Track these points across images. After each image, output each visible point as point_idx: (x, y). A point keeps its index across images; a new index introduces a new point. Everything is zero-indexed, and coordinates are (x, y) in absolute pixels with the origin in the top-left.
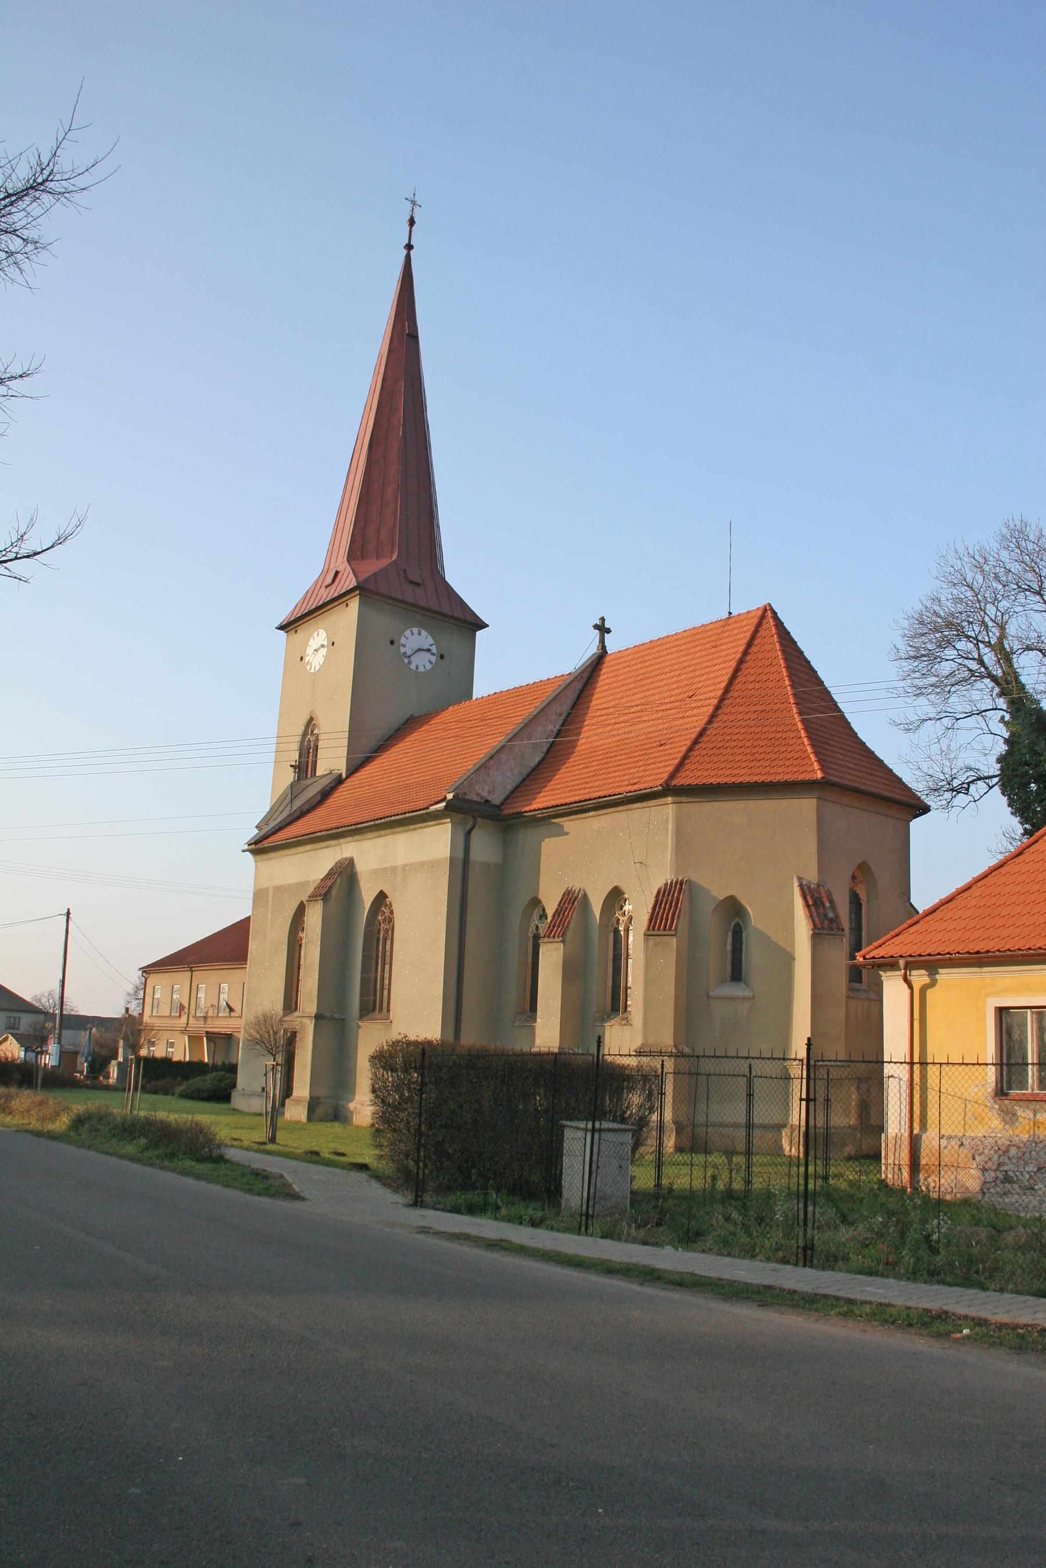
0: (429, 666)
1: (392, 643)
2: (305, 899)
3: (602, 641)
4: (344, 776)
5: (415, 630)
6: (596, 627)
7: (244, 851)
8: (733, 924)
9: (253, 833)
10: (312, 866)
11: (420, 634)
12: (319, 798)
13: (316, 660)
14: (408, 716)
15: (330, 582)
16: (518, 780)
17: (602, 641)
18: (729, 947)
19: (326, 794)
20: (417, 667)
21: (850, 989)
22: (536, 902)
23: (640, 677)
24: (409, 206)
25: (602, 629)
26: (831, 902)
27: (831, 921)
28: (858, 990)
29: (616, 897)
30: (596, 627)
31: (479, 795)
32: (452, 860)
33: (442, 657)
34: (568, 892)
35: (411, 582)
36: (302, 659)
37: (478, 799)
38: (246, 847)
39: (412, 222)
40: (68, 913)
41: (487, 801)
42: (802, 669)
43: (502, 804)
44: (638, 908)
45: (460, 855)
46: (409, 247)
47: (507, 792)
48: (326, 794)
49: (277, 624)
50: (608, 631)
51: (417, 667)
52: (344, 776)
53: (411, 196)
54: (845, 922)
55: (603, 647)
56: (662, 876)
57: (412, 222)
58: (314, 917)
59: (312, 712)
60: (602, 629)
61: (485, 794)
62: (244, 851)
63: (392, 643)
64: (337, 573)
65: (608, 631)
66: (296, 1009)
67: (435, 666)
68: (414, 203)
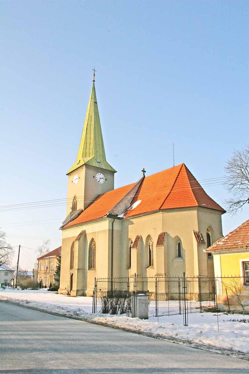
0: (103, 182)
1: (94, 177)
2: (74, 240)
4: (83, 210)
5: (99, 174)
6: (142, 171)
8: (178, 243)
9: (62, 225)
10: (75, 232)
11: (100, 174)
12: (77, 215)
15: (78, 163)
18: (177, 249)
19: (79, 214)
25: (144, 171)
26: (202, 236)
27: (202, 241)
29: (149, 237)
30: (142, 171)
31: (115, 213)
32: (109, 230)
33: (106, 180)
35: (98, 162)
36: (72, 182)
38: (60, 228)
39: (94, 75)
44: (155, 240)
45: (111, 228)
48: (79, 214)
50: (145, 172)
52: (83, 210)
54: (206, 241)
55: (144, 176)
56: (160, 232)
58: (77, 244)
59: (75, 195)
60: (144, 171)
63: (94, 177)
64: (80, 161)
65: (145, 172)
66: (73, 268)
68: (94, 70)
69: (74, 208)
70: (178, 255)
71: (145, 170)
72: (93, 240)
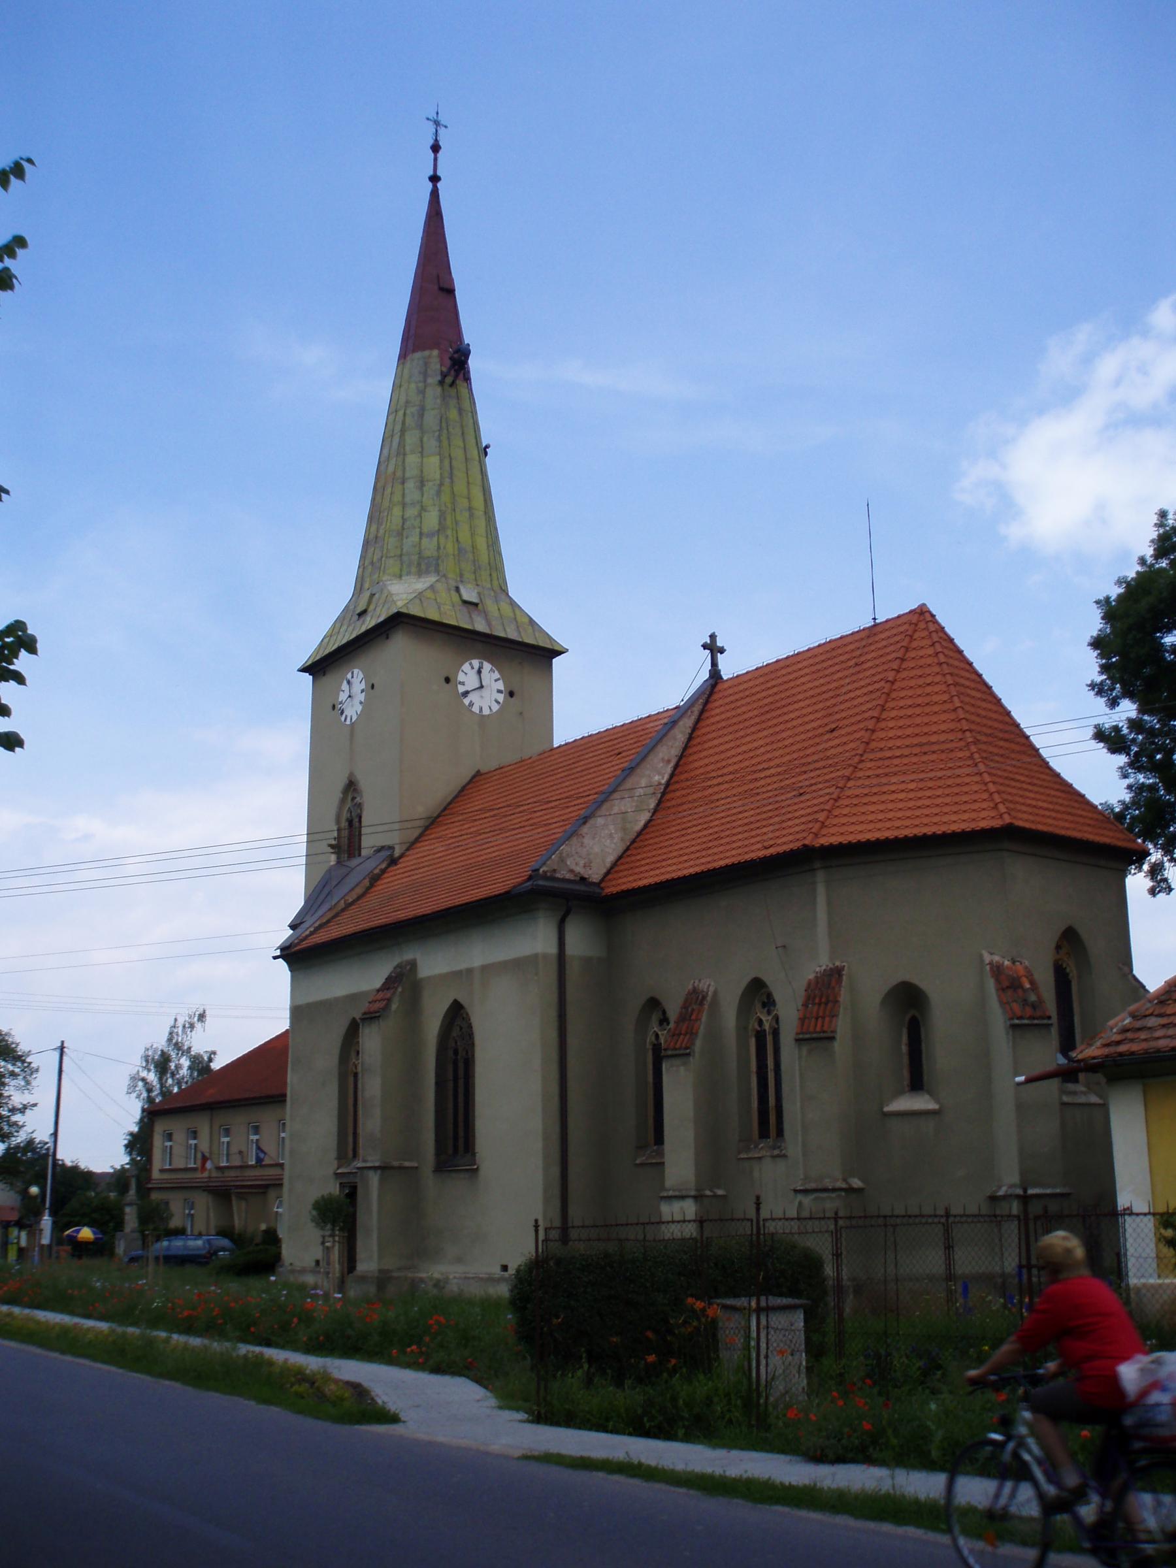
0: (496, 707)
2: (358, 1016)
3: (714, 664)
6: (705, 646)
7: (275, 958)
10: (364, 978)
13: (353, 711)
14: (473, 773)
16: (620, 848)
17: (714, 664)
18: (904, 1048)
20: (481, 709)
21: (1063, 1092)
22: (653, 1004)
23: (766, 709)
24: (431, 128)
25: (713, 648)
26: (1032, 982)
27: (1034, 1006)
28: (1075, 1093)
29: (758, 993)
30: (705, 646)
31: (572, 871)
33: (511, 694)
34: (695, 990)
37: (569, 876)
38: (278, 953)
39: (436, 148)
40: (62, 1049)
41: (583, 879)
42: (973, 685)
43: (602, 880)
46: (435, 179)
47: (608, 865)
49: (300, 665)
50: (722, 651)
51: (481, 709)
53: (433, 115)
54: (1051, 1007)
55: (715, 673)
57: (436, 148)
58: (372, 1041)
59: (351, 774)
60: (713, 648)
61: (578, 869)
62: (275, 958)
63: (447, 680)
64: (373, 595)
65: (722, 651)
66: (355, 1155)
67: (503, 707)
68: (437, 123)
70: (906, 1082)
71: (719, 644)
72: (457, 1013)
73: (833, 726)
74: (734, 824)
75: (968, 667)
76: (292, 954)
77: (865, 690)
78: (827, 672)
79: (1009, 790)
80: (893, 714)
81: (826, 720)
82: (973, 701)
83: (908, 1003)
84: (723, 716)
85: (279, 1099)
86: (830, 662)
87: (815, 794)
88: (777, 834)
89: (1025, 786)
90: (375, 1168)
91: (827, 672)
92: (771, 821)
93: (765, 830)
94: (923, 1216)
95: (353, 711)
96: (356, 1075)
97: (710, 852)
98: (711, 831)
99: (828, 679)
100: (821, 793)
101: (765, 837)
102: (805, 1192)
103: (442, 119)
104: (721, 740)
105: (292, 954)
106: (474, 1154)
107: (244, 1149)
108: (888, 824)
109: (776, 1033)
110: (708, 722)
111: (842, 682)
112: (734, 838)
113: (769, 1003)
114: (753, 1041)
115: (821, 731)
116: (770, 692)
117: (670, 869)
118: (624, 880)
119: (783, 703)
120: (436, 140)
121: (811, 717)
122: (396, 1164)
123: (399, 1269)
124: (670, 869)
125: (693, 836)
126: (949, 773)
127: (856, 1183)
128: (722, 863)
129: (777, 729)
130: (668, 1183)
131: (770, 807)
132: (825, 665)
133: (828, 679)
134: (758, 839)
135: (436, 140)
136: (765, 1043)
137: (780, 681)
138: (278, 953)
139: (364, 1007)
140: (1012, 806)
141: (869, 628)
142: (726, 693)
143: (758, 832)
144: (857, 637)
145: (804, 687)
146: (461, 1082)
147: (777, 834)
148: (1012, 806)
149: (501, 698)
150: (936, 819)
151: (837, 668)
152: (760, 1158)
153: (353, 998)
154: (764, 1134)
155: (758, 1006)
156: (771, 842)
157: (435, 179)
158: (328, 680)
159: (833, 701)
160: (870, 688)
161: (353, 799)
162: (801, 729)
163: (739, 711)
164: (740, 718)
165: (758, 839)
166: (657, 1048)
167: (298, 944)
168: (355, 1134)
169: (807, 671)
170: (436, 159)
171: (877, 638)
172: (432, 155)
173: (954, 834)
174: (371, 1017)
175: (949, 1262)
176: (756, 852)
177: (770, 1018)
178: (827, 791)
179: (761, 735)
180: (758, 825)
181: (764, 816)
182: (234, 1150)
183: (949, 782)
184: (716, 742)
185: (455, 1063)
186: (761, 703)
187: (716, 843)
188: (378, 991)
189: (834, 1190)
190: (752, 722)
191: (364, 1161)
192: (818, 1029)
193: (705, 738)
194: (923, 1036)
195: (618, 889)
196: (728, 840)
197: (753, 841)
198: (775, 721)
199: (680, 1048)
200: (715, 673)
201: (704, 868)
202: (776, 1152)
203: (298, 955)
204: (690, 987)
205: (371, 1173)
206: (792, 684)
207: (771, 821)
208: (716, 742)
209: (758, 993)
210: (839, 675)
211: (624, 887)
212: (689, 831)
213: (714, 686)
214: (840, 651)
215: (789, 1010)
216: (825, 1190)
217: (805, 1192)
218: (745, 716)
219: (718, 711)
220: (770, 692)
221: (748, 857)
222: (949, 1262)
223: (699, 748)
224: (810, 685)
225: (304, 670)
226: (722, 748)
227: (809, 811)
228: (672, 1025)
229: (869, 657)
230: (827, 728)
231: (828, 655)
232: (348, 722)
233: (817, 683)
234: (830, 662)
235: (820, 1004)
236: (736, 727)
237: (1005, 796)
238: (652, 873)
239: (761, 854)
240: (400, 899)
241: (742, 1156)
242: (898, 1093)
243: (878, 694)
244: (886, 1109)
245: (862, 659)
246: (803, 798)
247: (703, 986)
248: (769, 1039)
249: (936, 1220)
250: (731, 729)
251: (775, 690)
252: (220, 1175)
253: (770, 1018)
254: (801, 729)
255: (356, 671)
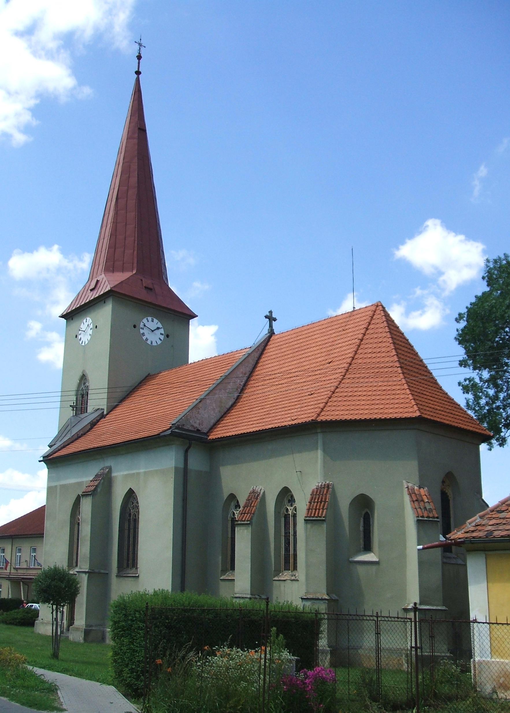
0: (159, 342)
1: (135, 326)
3: (271, 326)
4: (105, 413)
5: (150, 319)
7: (40, 461)
8: (364, 513)
9: (45, 450)
11: (153, 321)
13: (85, 338)
14: (147, 374)
15: (93, 287)
16: (219, 416)
17: (271, 326)
18: (361, 529)
19: (93, 424)
20: (152, 343)
21: (444, 557)
22: (232, 497)
23: (297, 350)
24: (137, 47)
25: (271, 318)
28: (449, 558)
29: (286, 495)
31: (192, 426)
32: (176, 468)
33: (168, 336)
34: (254, 492)
36: (76, 336)
37: (191, 428)
38: (42, 459)
39: (139, 57)
41: (198, 430)
42: (403, 344)
43: (208, 432)
44: (302, 505)
45: (181, 466)
46: (138, 73)
47: (212, 424)
48: (93, 424)
49: (60, 314)
50: (275, 320)
51: (152, 343)
52: (105, 413)
53: (138, 40)
55: (272, 333)
56: (315, 481)
57: (139, 57)
58: (86, 506)
59: (84, 371)
60: (271, 318)
61: (196, 425)
62: (40, 461)
63: (135, 326)
65: (275, 320)
66: (77, 566)
67: (163, 342)
68: (140, 45)
69: (80, 405)
70: (362, 546)
71: (274, 316)
72: (131, 495)
73: (330, 361)
74: (277, 407)
75: (401, 335)
76: (51, 460)
77: (347, 343)
78: (328, 333)
79: (420, 399)
80: (361, 356)
81: (326, 357)
82: (403, 353)
83: (364, 506)
84: (274, 353)
85: (40, 535)
86: (330, 328)
87: (319, 395)
88: (299, 413)
89: (429, 397)
90: (85, 572)
91: (328, 333)
92: (296, 407)
93: (293, 411)
94: (365, 616)
95: (85, 338)
96: (79, 524)
97: (264, 420)
98: (265, 410)
99: (328, 337)
100: (323, 394)
101: (292, 415)
102: (307, 599)
103: (143, 43)
104: (272, 365)
105: (51, 460)
106: (137, 568)
107: (28, 560)
108: (356, 412)
109: (295, 516)
110: (266, 355)
111: (336, 339)
112: (277, 414)
113: (292, 501)
114: (283, 519)
115: (324, 362)
116: (299, 342)
117: (243, 428)
118: (219, 432)
119: (305, 347)
120: (139, 53)
121: (319, 355)
122: (96, 571)
123: (96, 626)
124: (243, 428)
125: (256, 412)
126: (389, 388)
127: (334, 597)
128: (270, 426)
129: (301, 360)
130: (237, 590)
131: (296, 400)
132: (328, 329)
133: (328, 337)
134: (289, 415)
135: (139, 53)
136: (286, 520)
137: (304, 336)
138: (42, 459)
139: (84, 489)
140: (421, 407)
141: (351, 312)
142: (276, 341)
143: (289, 412)
144: (344, 316)
145: (317, 340)
146: (132, 531)
147: (299, 413)
148: (421, 407)
149: (162, 337)
150: (381, 411)
151: (334, 331)
152: (285, 580)
153: (80, 484)
154: (287, 568)
155: (286, 501)
156: (295, 418)
157: (138, 73)
158: (74, 324)
159: (331, 348)
160: (350, 342)
161: (84, 383)
162: (314, 361)
163: (283, 351)
164: (282, 354)
165: (289, 415)
166: (233, 520)
167: (52, 455)
168: (77, 554)
169: (318, 332)
170: (139, 63)
171: (354, 317)
172: (137, 61)
173: (391, 419)
174: (85, 495)
175: (378, 642)
176: (287, 422)
177: (292, 508)
178: (326, 393)
179: (293, 363)
180: (289, 408)
181: (293, 404)
182: (23, 560)
183: (389, 392)
184: (270, 366)
185: (129, 521)
186: (293, 347)
187: (267, 416)
188: (91, 481)
189: (322, 599)
190: (289, 356)
191: (80, 568)
192: (316, 515)
193: (264, 363)
194: (371, 523)
195: (217, 437)
196: (273, 415)
197: (286, 416)
198: (300, 357)
199: (244, 521)
200: (272, 333)
201: (260, 428)
202: (293, 578)
203: (54, 461)
204: (251, 489)
205: (84, 575)
206: (310, 338)
207: (296, 407)
208: (270, 366)
209: (286, 495)
210: (334, 335)
211: (219, 436)
212: (254, 409)
213: (270, 337)
214: (335, 323)
215: (302, 505)
216: (318, 599)
217: (307, 599)
218: (285, 353)
219: (271, 350)
220: (299, 342)
221: (283, 424)
222: (378, 642)
223: (261, 368)
224: (319, 339)
225: (62, 316)
226: (273, 369)
227: (316, 402)
228: (241, 509)
229: (349, 326)
230: (327, 362)
231: (329, 325)
232: (83, 344)
233: (322, 338)
234: (330, 328)
235: (318, 502)
236: (280, 359)
237: (418, 402)
238: (234, 429)
239: (290, 423)
240: (106, 435)
241: (275, 579)
242: (358, 552)
243: (354, 345)
244: (351, 559)
245: (347, 327)
246: (312, 396)
247: (258, 489)
248: (291, 519)
249: (372, 618)
250: (277, 360)
251: (301, 341)
252: (15, 572)
253: (292, 508)
254: (314, 361)
255: (88, 318)
